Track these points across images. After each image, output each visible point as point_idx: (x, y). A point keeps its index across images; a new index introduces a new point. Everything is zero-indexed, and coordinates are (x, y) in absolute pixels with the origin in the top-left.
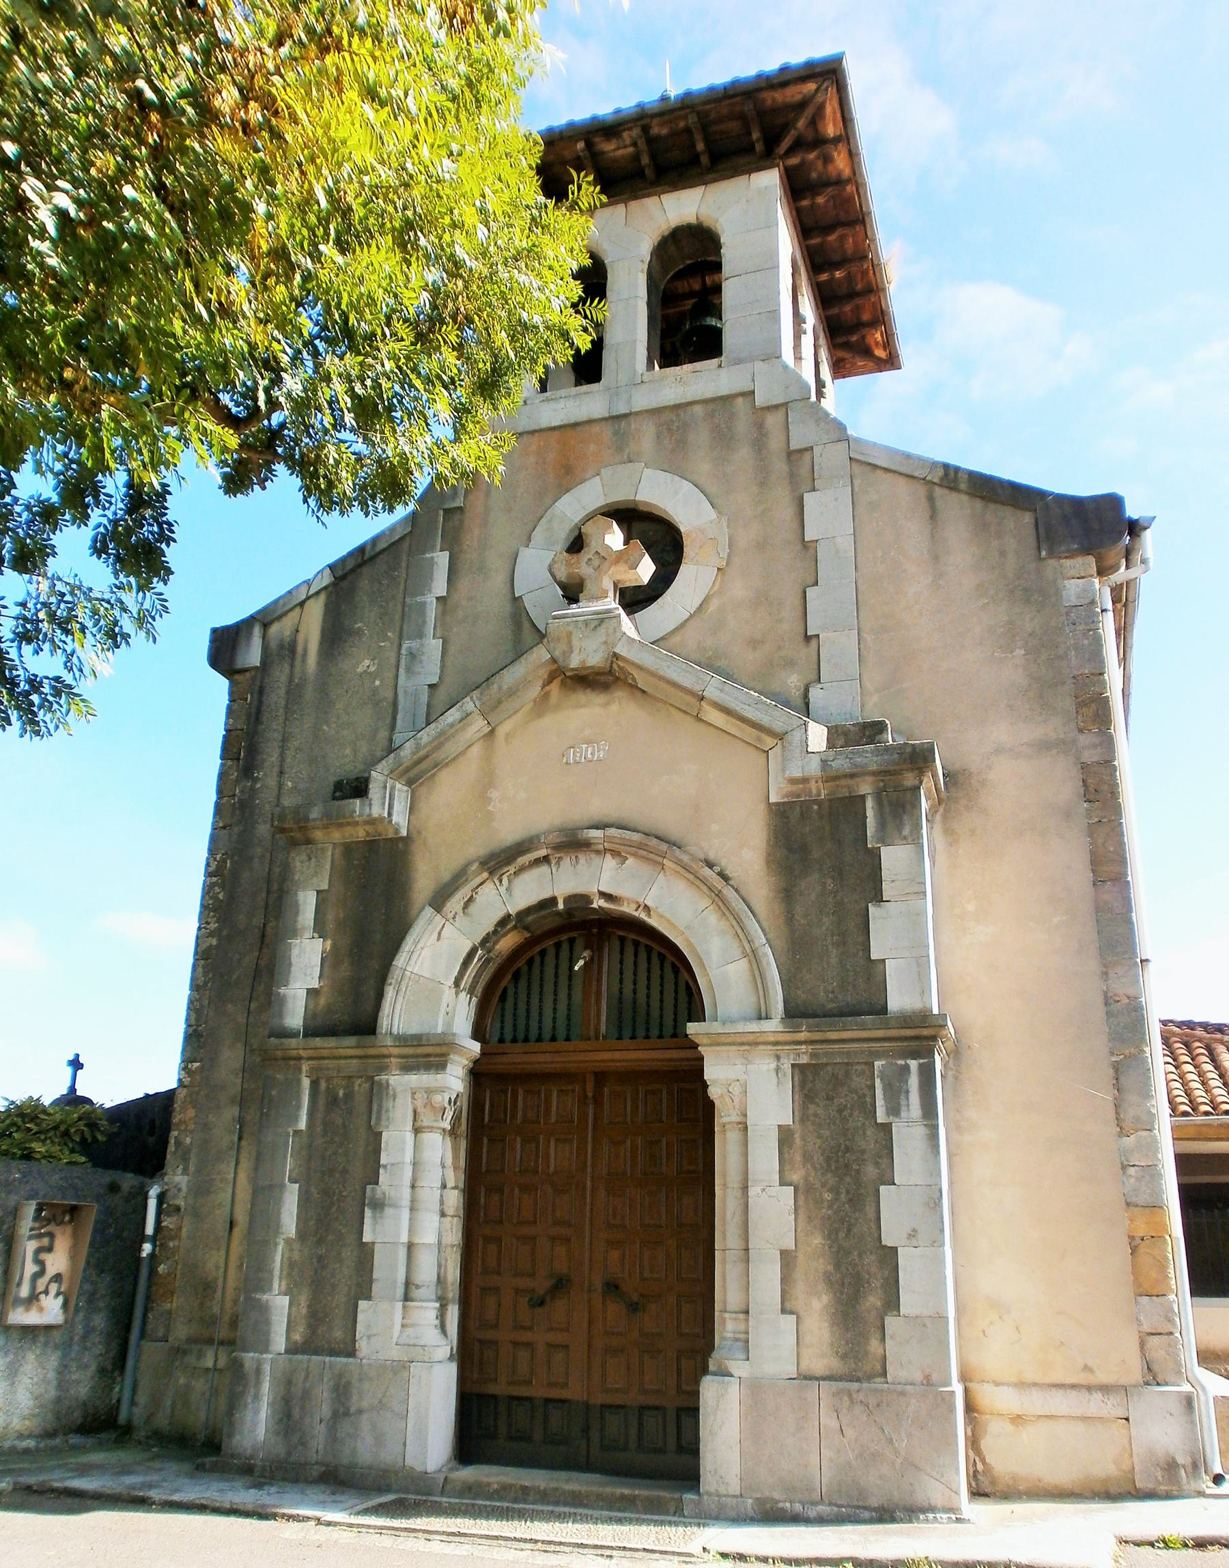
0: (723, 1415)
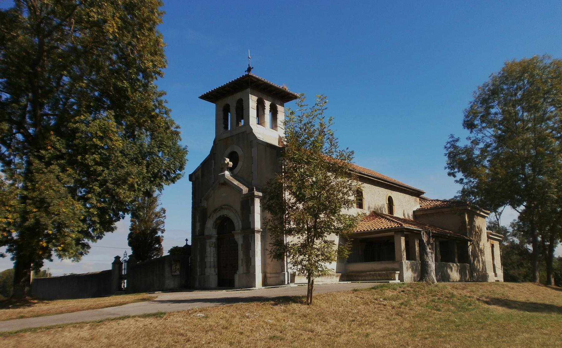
0: (237, 277)
